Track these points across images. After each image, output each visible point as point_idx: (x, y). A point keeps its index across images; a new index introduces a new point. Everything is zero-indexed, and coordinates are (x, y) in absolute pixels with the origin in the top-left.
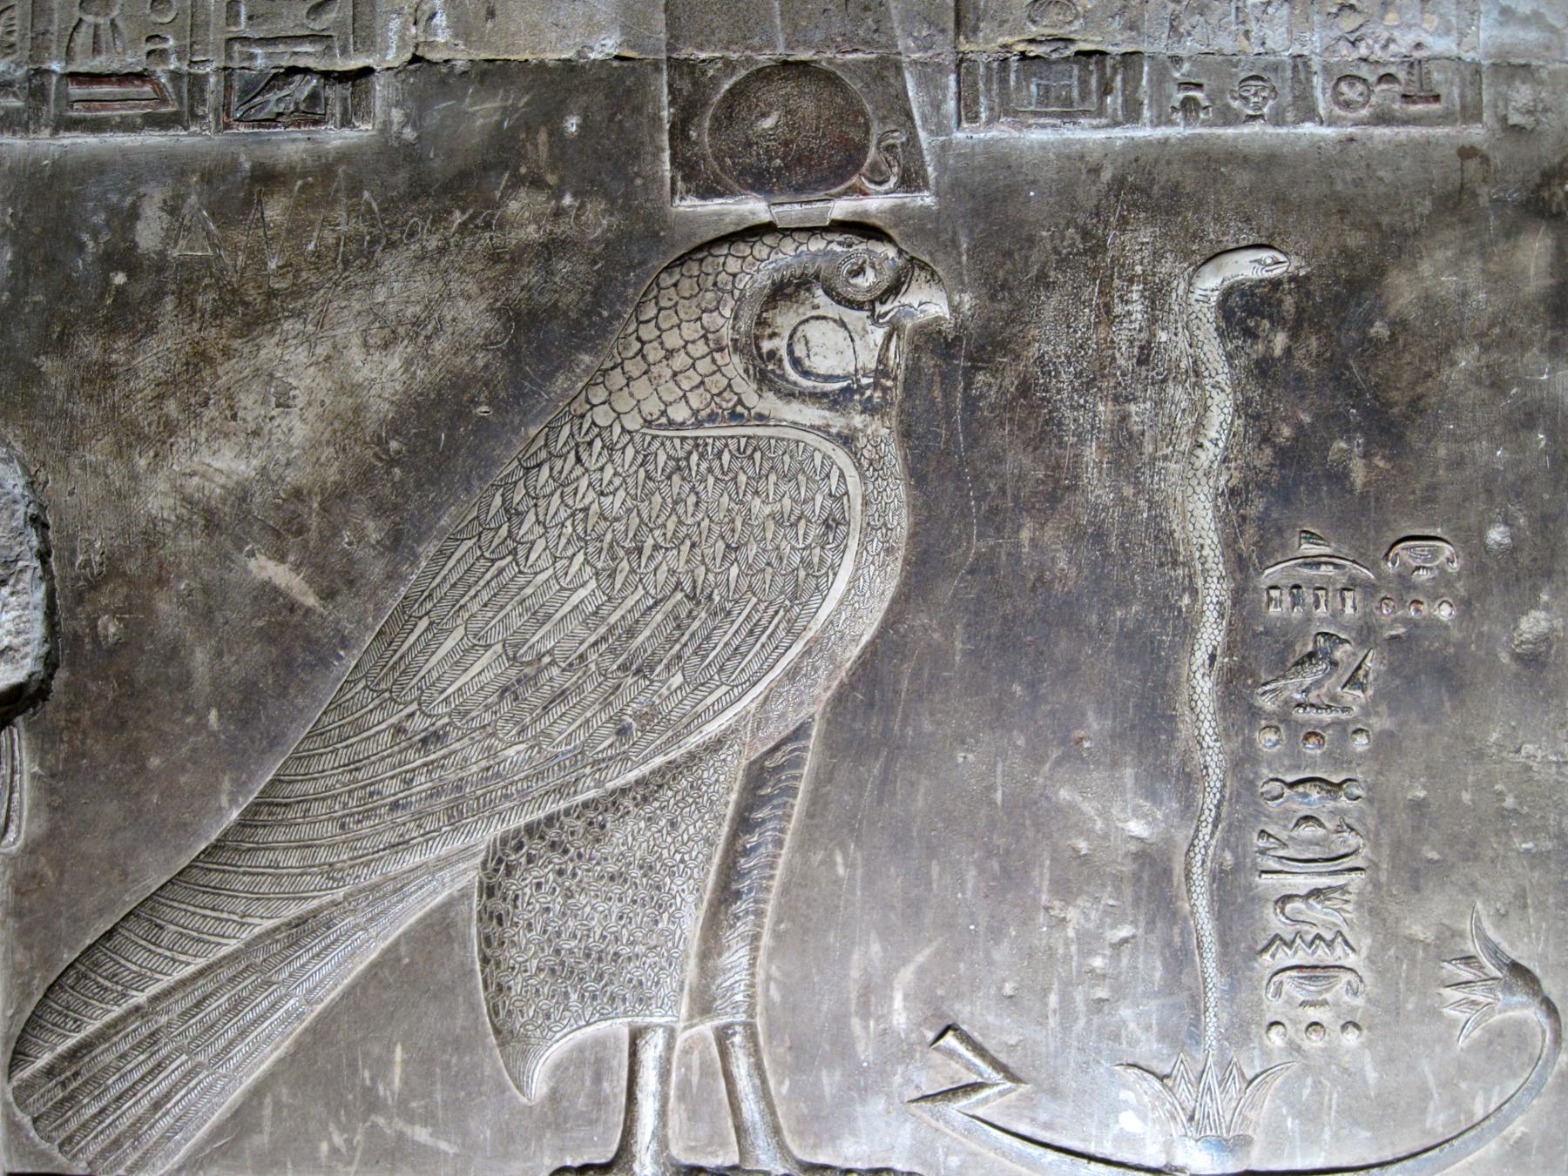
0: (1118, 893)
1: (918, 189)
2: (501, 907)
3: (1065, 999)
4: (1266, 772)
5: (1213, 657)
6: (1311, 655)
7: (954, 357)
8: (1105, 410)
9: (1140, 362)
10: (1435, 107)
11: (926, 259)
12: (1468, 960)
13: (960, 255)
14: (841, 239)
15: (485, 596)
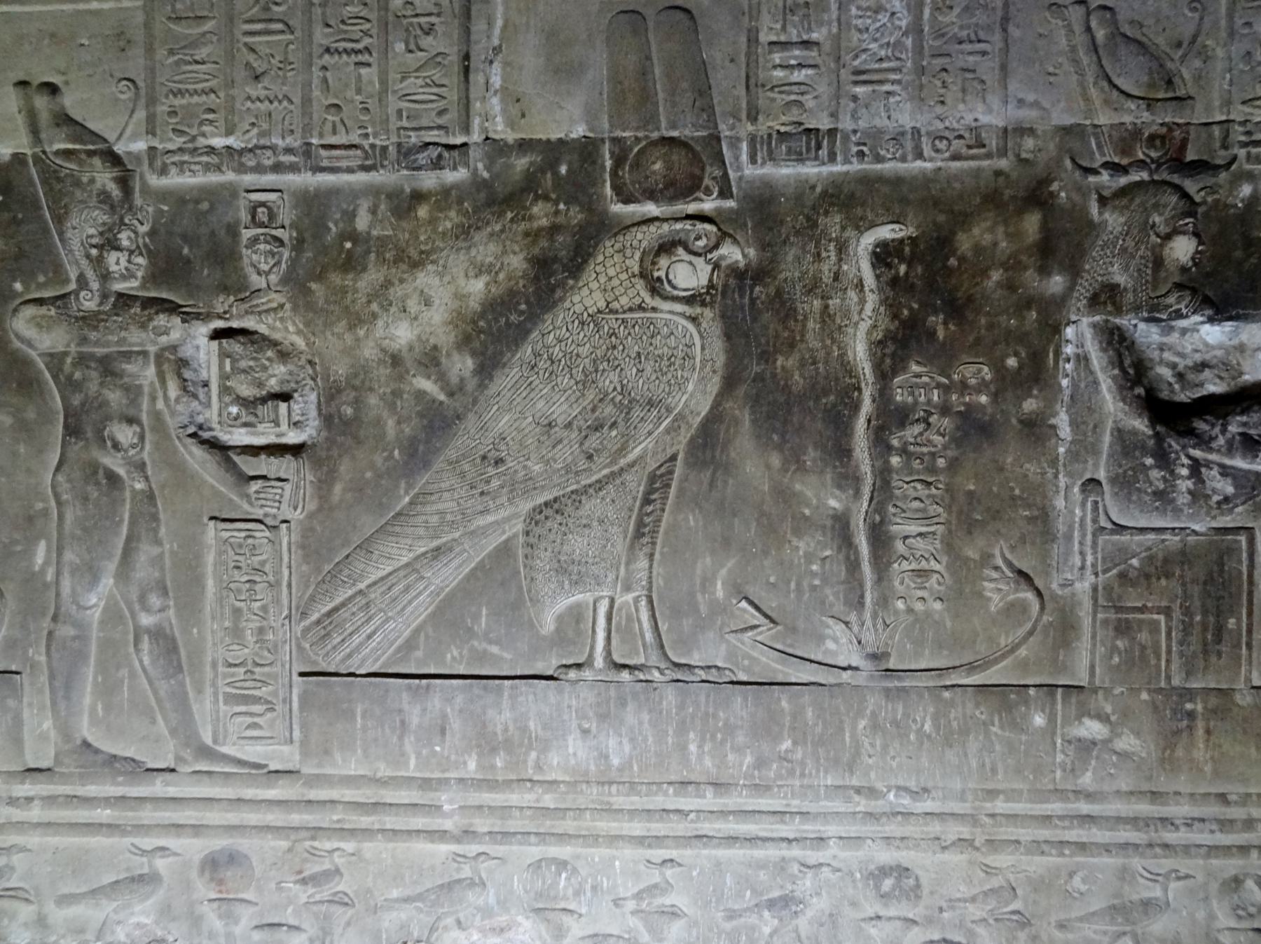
0: (824, 534)
2: (532, 540)
3: (798, 584)
4: (895, 476)
5: (869, 421)
6: (918, 420)
10: (983, 150)
11: (731, 232)
12: (996, 568)
15: (524, 395)
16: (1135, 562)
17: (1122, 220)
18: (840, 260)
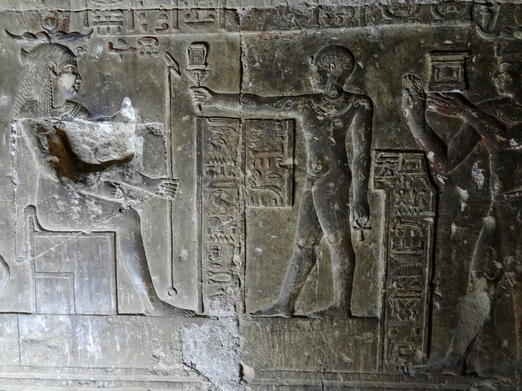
16: (52, 249)
17: (34, 65)
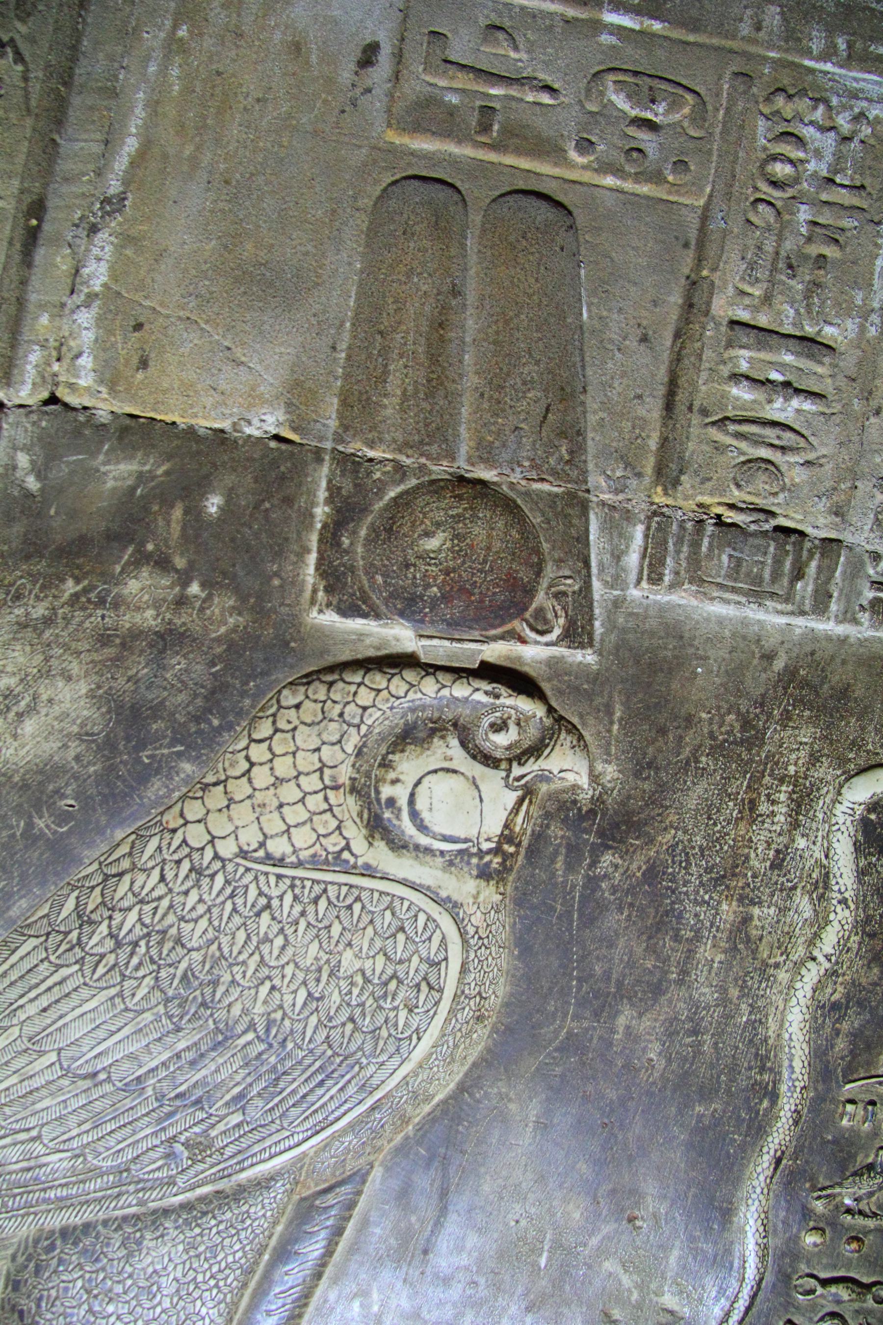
1: (582, 646)
5: (778, 1161)
7: (588, 831)
8: (728, 910)
9: (773, 867)
11: (575, 720)
13: (612, 723)
14: (489, 688)
18: (795, 825)
